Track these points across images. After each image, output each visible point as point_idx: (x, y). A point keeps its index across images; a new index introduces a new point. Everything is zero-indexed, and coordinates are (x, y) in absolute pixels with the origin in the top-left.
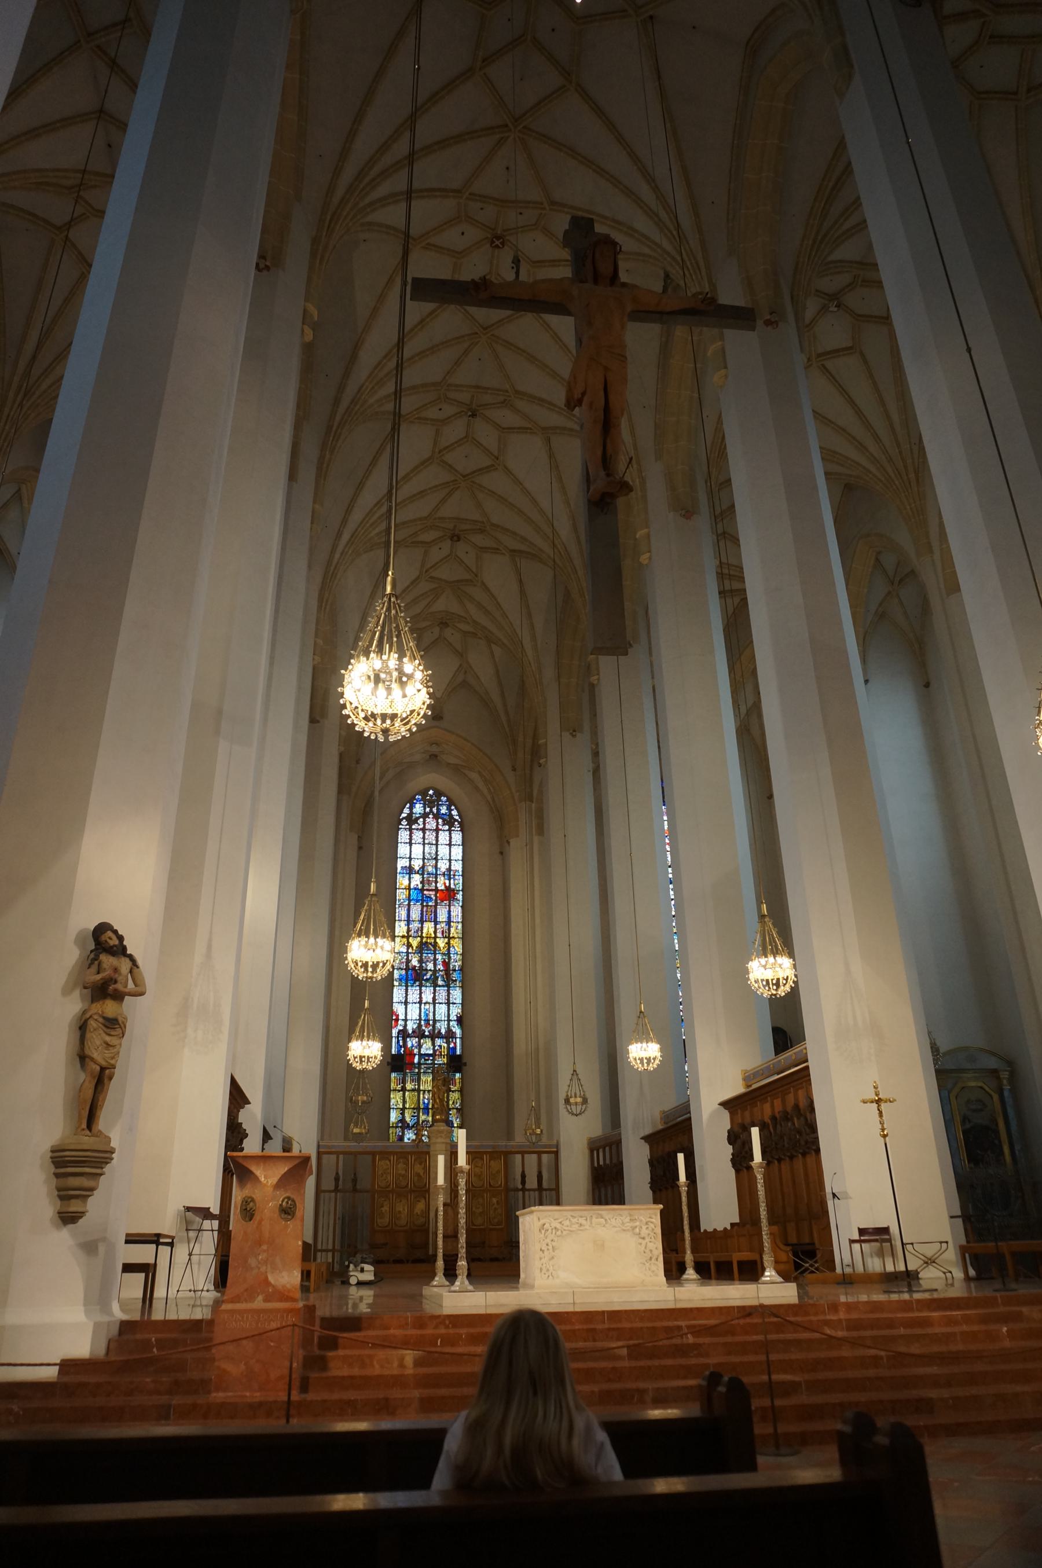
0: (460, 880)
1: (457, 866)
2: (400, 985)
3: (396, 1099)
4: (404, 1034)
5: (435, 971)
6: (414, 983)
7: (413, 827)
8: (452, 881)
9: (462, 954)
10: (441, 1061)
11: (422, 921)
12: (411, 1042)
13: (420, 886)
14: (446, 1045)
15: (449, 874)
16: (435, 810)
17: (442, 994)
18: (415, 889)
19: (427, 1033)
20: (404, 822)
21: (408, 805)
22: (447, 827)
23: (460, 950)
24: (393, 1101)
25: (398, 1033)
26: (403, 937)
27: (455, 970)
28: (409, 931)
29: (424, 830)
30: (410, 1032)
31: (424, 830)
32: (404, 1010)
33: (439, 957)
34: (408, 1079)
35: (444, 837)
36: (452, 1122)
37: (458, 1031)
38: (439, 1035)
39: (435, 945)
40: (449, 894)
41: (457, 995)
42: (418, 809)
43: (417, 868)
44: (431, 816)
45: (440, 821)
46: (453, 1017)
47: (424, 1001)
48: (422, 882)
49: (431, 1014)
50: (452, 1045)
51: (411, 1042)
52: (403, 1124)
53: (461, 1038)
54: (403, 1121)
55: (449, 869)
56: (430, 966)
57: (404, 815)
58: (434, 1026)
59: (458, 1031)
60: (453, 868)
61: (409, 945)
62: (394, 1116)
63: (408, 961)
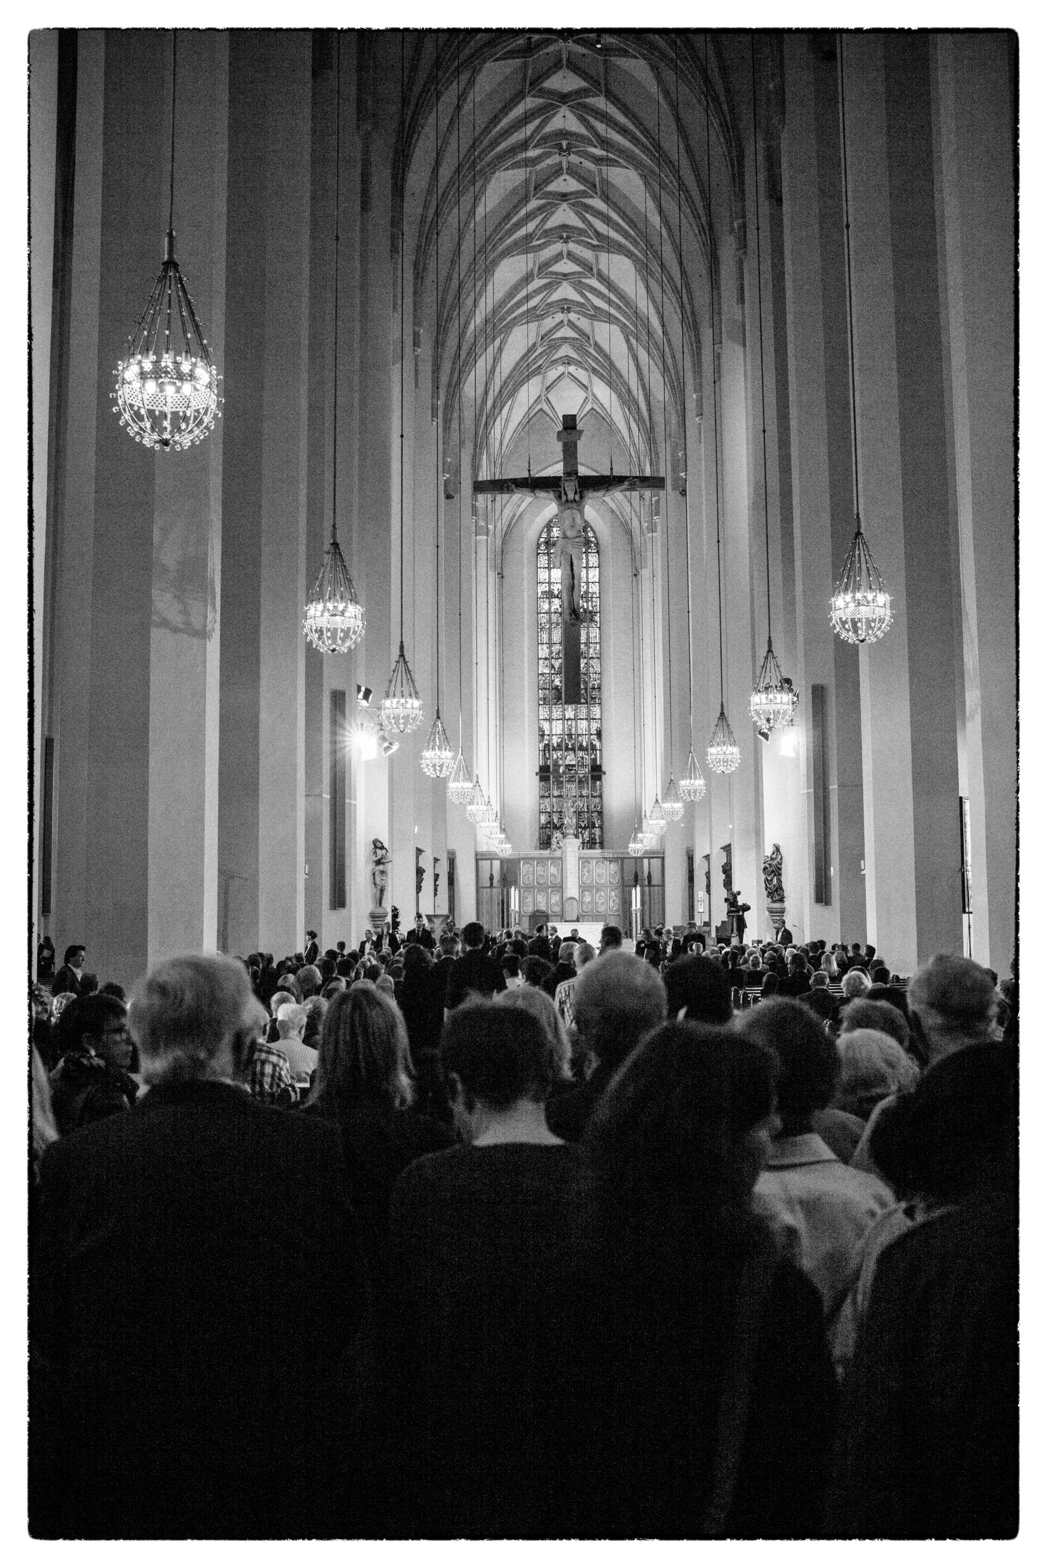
8: (590, 603)
10: (584, 771)
18: (555, 613)
26: (546, 659)
28: (551, 653)
30: (555, 745)
43: (556, 592)
47: (567, 717)
49: (573, 729)
50: (593, 756)
55: (587, 592)
57: (542, 540)
60: (590, 590)
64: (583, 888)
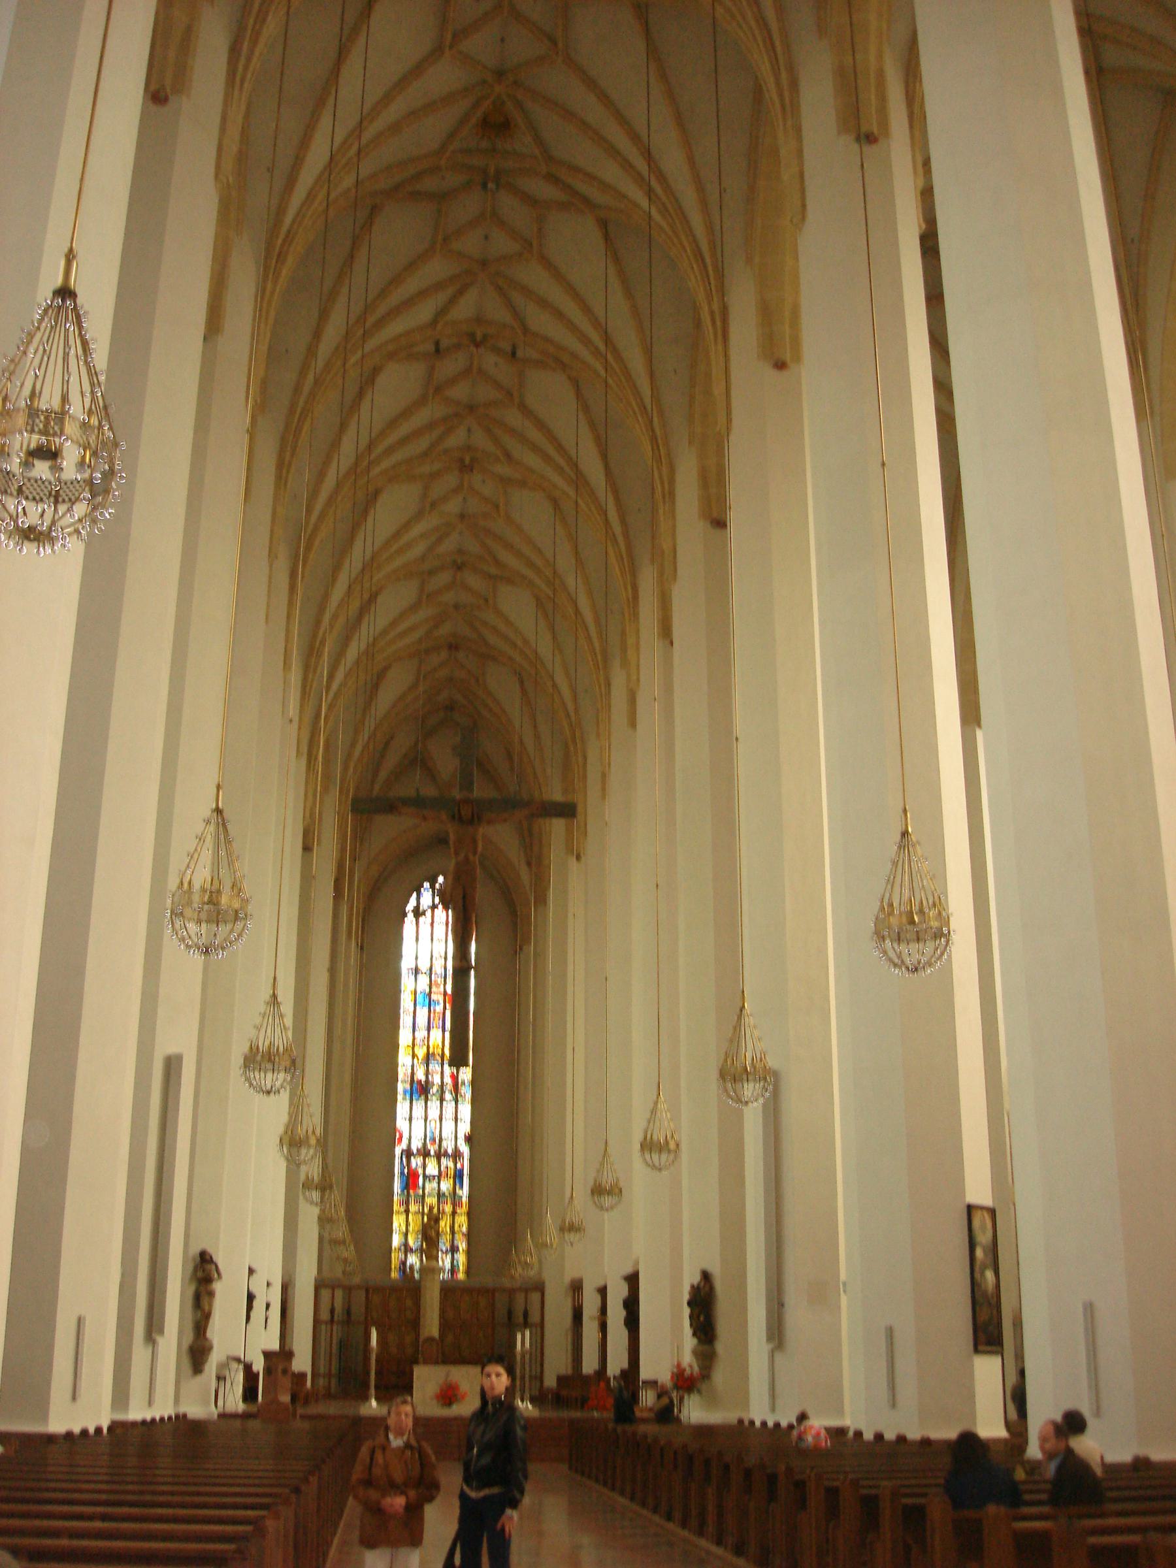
2: (404, 1099)
3: (398, 1222)
4: (408, 1153)
6: (420, 1096)
12: (416, 1162)
14: (451, 1164)
17: (449, 1107)
19: (432, 1153)
21: (415, 895)
24: (395, 1225)
25: (403, 1151)
27: (463, 1083)
30: (414, 1149)
32: (408, 1125)
36: (458, 1248)
38: (446, 1154)
41: (465, 1110)
46: (461, 1136)
51: (416, 1162)
52: (407, 1249)
53: (471, 1160)
54: (406, 1244)
59: (465, 1149)
61: (414, 1056)
62: (396, 1240)
63: (413, 1074)
64: (444, 1325)
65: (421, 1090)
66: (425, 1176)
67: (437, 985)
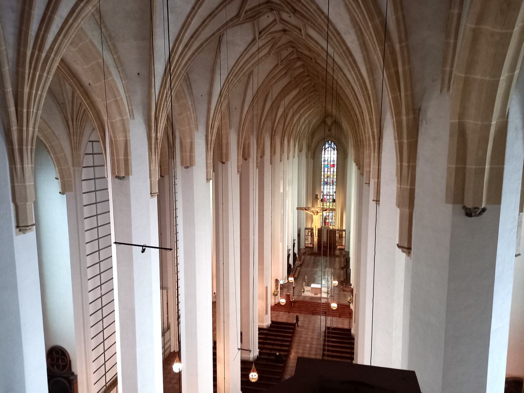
0: (336, 162)
1: (335, 159)
5: (330, 182)
7: (326, 150)
9: (336, 179)
11: (327, 172)
12: (325, 197)
13: (327, 164)
15: (334, 161)
16: (330, 146)
17: (331, 187)
20: (324, 149)
22: (333, 150)
23: (335, 178)
29: (328, 151)
31: (328, 151)
33: (331, 179)
34: (324, 203)
35: (332, 152)
37: (334, 194)
38: (331, 195)
39: (330, 177)
40: (333, 165)
41: (335, 187)
42: (327, 146)
44: (330, 147)
45: (332, 149)
48: (328, 163)
51: (325, 197)
55: (333, 160)
56: (329, 181)
58: (330, 194)
59: (334, 194)
65: (327, 183)
66: (327, 199)
67: (329, 163)
